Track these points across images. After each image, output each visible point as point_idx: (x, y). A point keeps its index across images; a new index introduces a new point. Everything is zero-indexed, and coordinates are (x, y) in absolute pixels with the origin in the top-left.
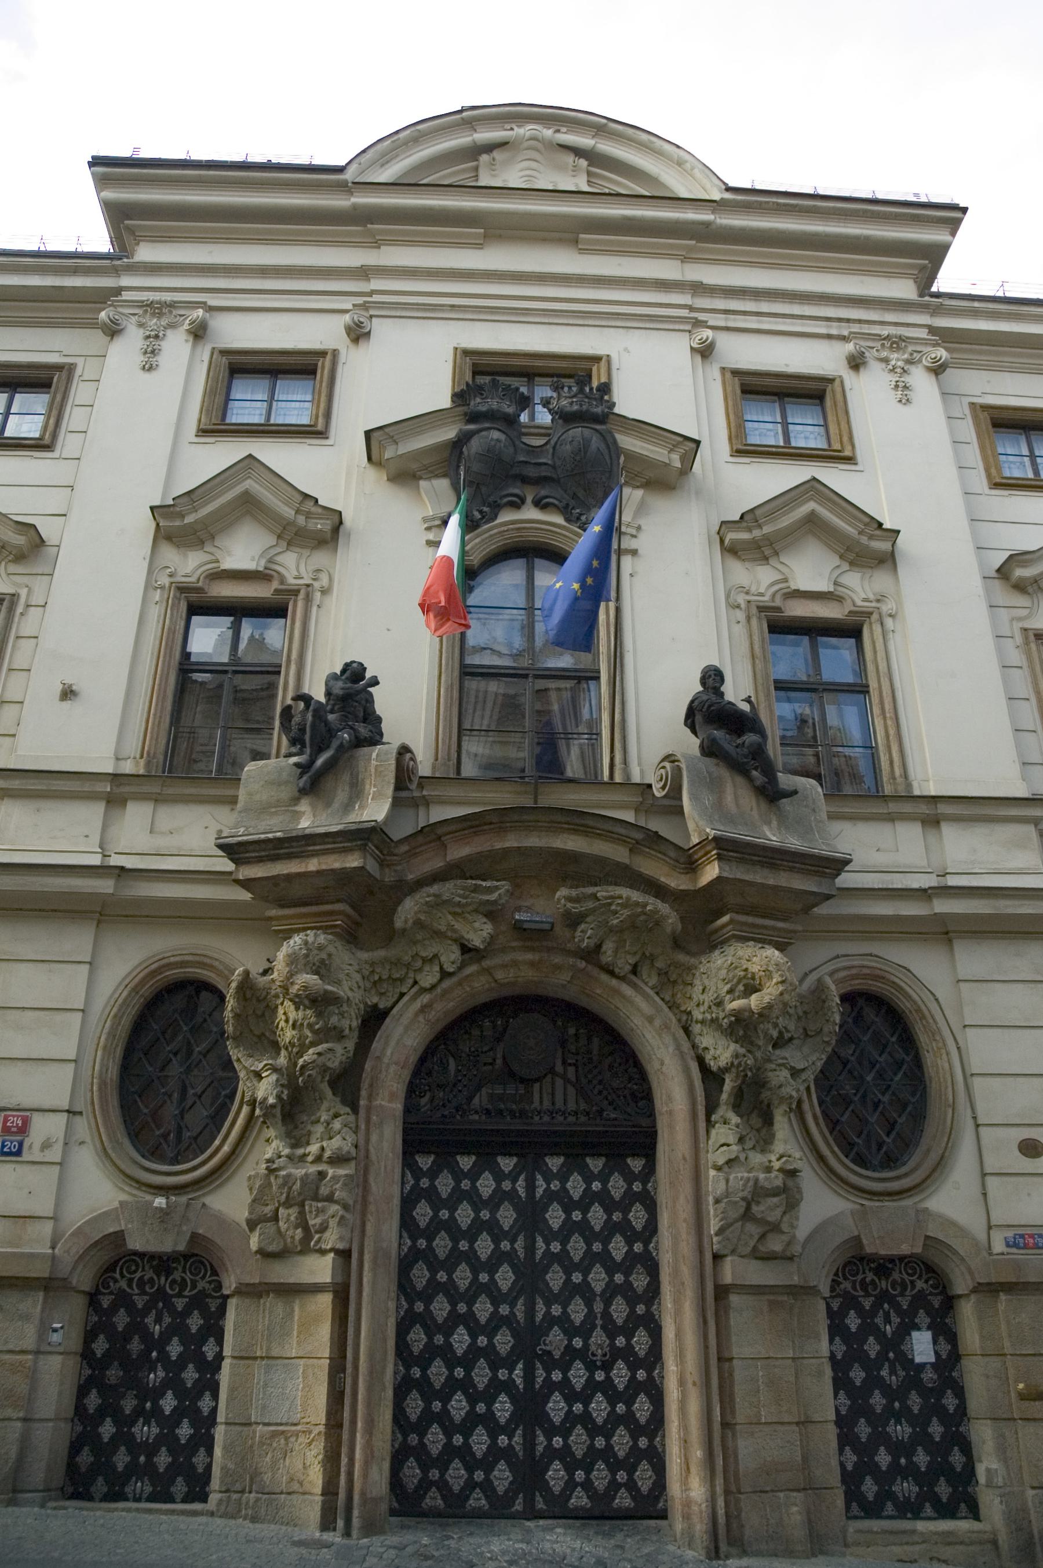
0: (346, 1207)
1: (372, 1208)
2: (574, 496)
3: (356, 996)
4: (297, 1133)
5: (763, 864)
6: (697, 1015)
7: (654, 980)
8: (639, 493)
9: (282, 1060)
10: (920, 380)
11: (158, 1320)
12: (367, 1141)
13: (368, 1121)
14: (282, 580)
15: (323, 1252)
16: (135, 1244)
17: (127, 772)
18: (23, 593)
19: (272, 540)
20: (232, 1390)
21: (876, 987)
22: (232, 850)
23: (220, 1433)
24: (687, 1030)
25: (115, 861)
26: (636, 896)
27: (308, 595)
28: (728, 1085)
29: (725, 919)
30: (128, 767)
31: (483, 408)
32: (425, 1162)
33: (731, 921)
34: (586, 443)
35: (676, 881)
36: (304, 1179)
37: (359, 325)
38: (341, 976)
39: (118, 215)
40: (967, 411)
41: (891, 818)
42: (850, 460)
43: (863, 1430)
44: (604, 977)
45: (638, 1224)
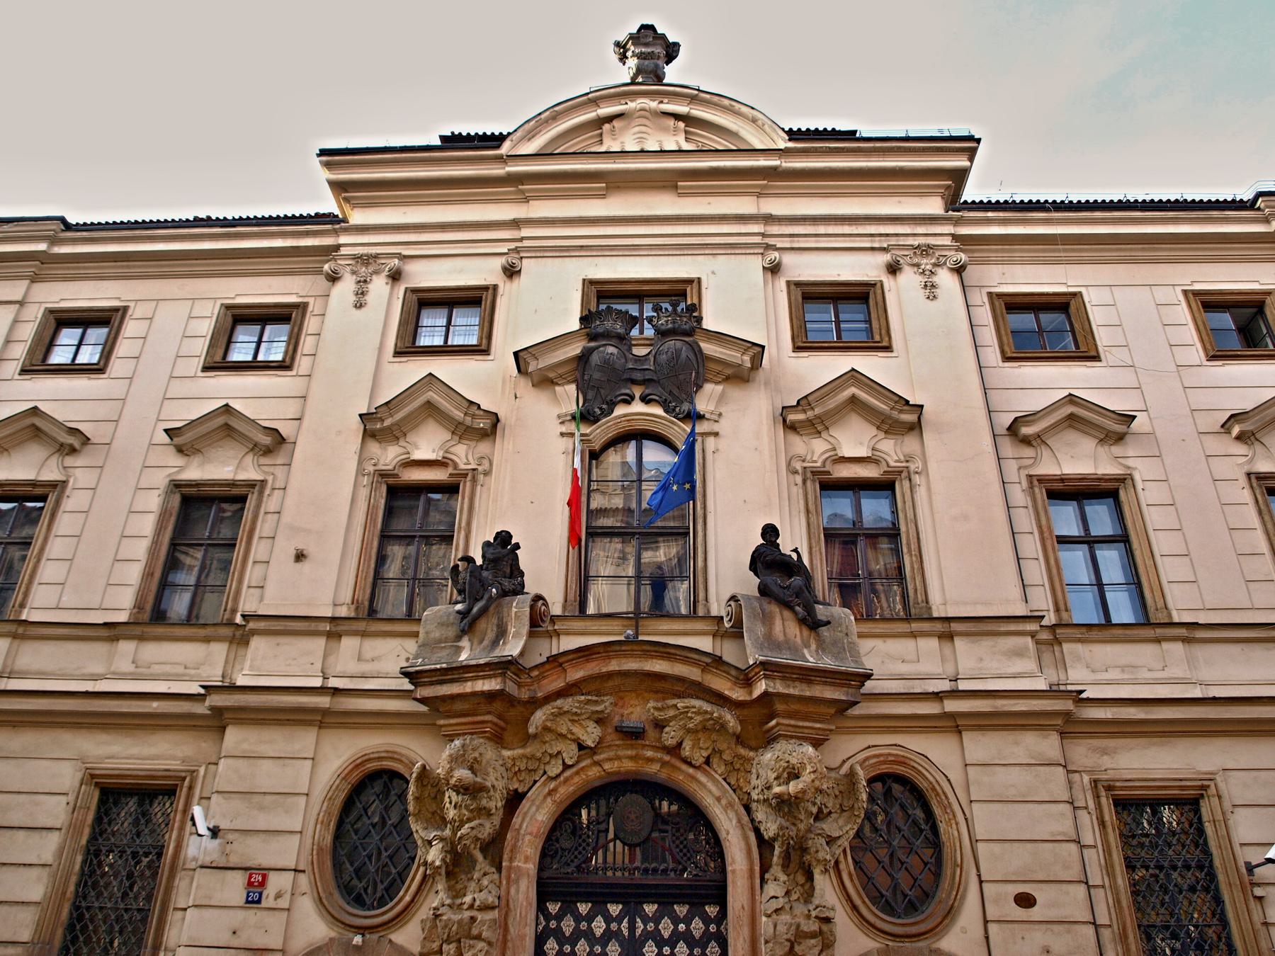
0: (490, 944)
1: (510, 944)
2: (671, 393)
3: (500, 784)
4: (459, 886)
5: (801, 680)
6: (755, 797)
7: (722, 769)
8: (720, 388)
9: (447, 832)
10: (945, 279)
12: (508, 893)
13: (509, 878)
14: (456, 466)
17: (343, 615)
18: (270, 479)
19: (448, 436)
21: (900, 770)
22: (413, 676)
24: (747, 808)
25: (333, 683)
26: (707, 707)
27: (474, 477)
28: (777, 852)
29: (773, 723)
30: (343, 612)
31: (600, 330)
32: (553, 908)
33: (778, 724)
34: (678, 352)
35: (738, 694)
36: (460, 922)
37: (512, 266)
38: (491, 770)
39: (339, 187)
40: (986, 299)
41: (913, 635)
42: (888, 348)
44: (684, 767)
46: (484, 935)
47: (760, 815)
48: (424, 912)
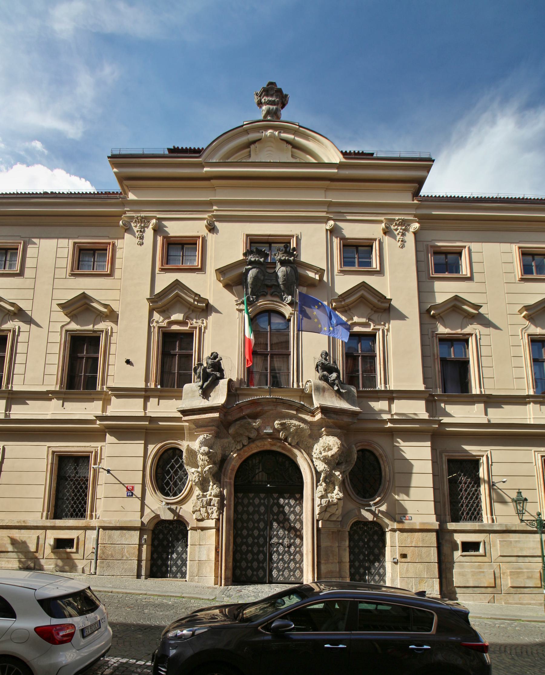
6: (314, 456)
9: (200, 470)
11: (171, 536)
15: (212, 519)
16: (163, 517)
20: (191, 553)
23: (188, 562)
26: (297, 423)
28: (323, 475)
43: (357, 564)
45: (298, 512)
46: (216, 505)
47: (315, 463)
48: (194, 497)
